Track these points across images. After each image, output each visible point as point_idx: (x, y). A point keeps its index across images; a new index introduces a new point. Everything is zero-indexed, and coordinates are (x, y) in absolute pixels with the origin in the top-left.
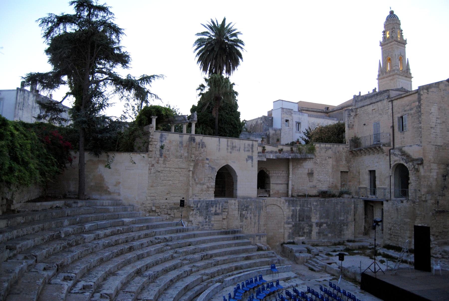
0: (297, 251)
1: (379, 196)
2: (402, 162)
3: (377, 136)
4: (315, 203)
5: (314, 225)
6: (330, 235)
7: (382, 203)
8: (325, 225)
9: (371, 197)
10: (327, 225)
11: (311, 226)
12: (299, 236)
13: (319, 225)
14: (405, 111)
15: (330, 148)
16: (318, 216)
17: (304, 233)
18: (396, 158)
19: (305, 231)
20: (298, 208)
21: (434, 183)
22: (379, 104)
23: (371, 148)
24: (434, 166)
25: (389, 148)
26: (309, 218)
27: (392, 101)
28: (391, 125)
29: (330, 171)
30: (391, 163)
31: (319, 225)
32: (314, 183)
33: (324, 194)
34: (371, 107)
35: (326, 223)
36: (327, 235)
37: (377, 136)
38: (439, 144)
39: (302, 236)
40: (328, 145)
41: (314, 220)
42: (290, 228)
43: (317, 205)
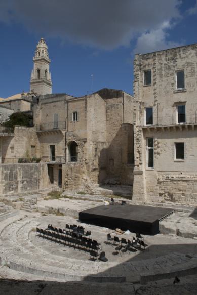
0: (13, 201)
1: (57, 161)
2: (74, 140)
3: (56, 123)
4: (19, 168)
5: (19, 182)
6: (28, 188)
7: (60, 166)
8: (25, 182)
9: (51, 162)
10: (27, 182)
11: (17, 183)
12: (10, 191)
13: (23, 182)
14: (77, 109)
15: (25, 129)
16: (21, 176)
17: (13, 188)
18: (70, 138)
19: (14, 187)
20: (9, 171)
21: (91, 152)
22: (59, 103)
23: (50, 132)
24: (92, 143)
25: (65, 131)
26: (16, 177)
27: (68, 102)
28: (67, 116)
29: (25, 145)
30: (67, 140)
31: (23, 182)
32: (14, 154)
33: (21, 161)
34: (53, 104)
35: (26, 180)
36: (27, 188)
37: (56, 123)
38: (94, 130)
39: (12, 191)
40: (24, 128)
41: (19, 179)
42: (4, 186)
43: (20, 169)
